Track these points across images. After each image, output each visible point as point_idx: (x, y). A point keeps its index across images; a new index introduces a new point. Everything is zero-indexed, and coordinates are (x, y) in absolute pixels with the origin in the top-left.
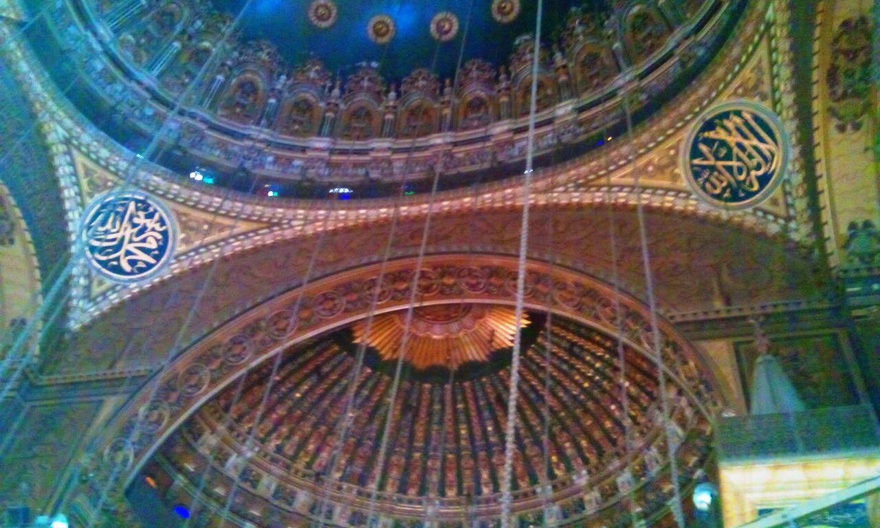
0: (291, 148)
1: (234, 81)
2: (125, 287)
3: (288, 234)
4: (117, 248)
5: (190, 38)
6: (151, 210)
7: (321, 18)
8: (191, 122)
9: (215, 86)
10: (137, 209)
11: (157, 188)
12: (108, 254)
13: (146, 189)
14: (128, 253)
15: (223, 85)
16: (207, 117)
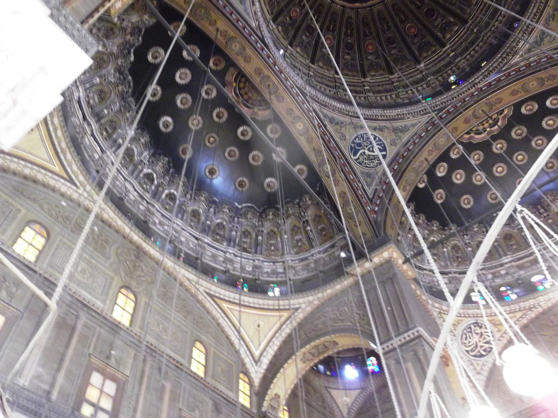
0: (496, 267)
1: (449, 248)
2: (487, 362)
3: (540, 310)
4: (476, 346)
5: (427, 239)
6: (480, 324)
7: (469, 203)
8: (450, 275)
9: (446, 254)
10: (475, 326)
11: (477, 314)
12: (474, 351)
13: (475, 317)
14: (481, 347)
15: (448, 251)
16: (455, 270)
